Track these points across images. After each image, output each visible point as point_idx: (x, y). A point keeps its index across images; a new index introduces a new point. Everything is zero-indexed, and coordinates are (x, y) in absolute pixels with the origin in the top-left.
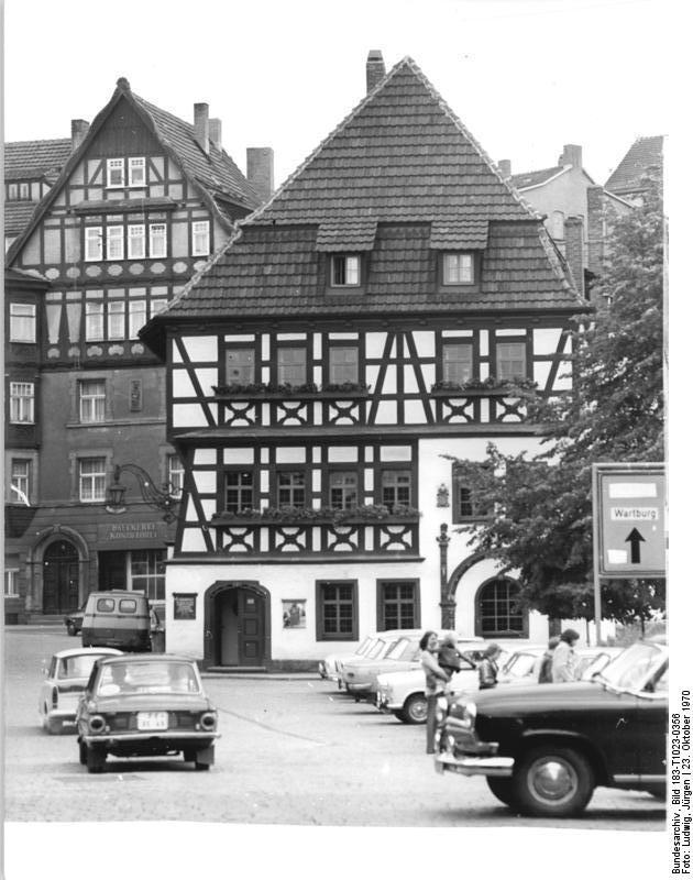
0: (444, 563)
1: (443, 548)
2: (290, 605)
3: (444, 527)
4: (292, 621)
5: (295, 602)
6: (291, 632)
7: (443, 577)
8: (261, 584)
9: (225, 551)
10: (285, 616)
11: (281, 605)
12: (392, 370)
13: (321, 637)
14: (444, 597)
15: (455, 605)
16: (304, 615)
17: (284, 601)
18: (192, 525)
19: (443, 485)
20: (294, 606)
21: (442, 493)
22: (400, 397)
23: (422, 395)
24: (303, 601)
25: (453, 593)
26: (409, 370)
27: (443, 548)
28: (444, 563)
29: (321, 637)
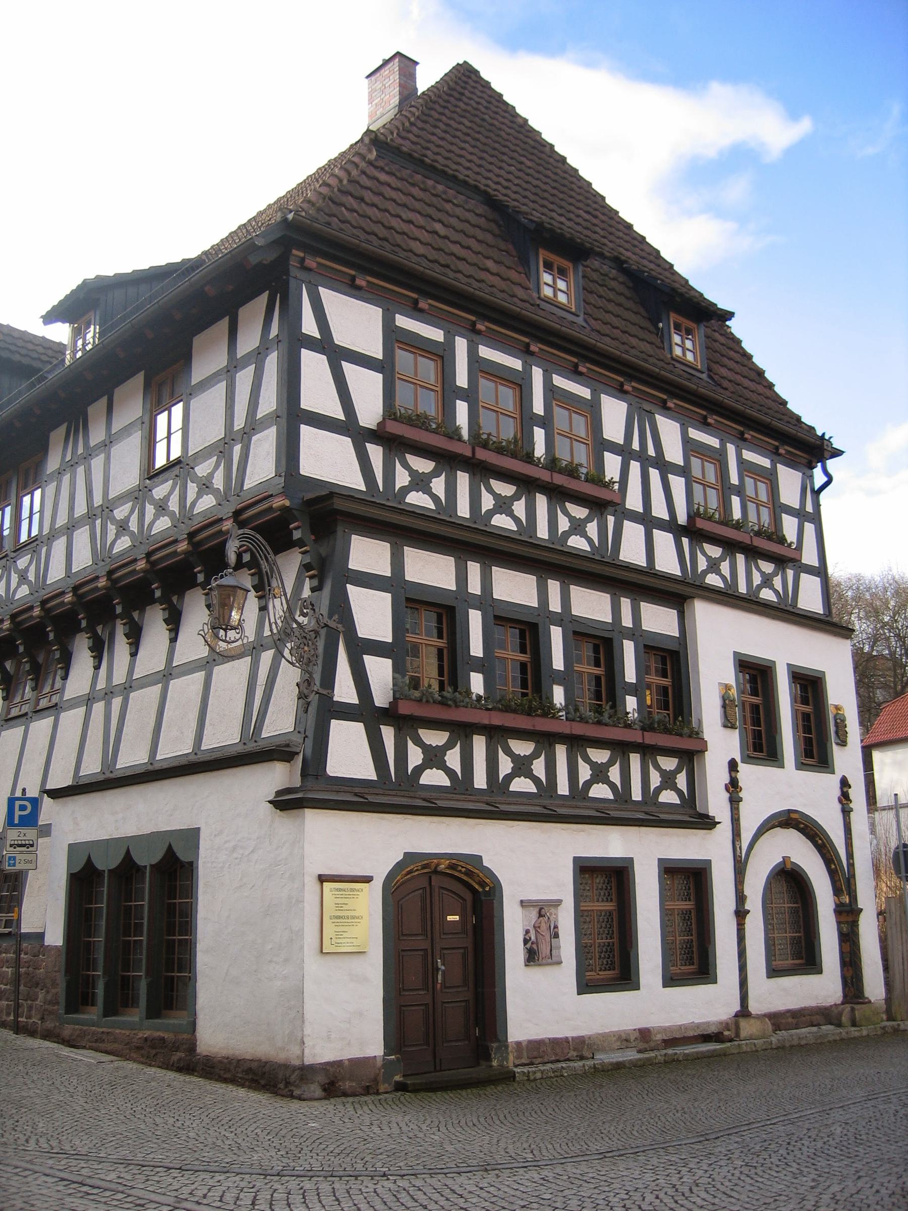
1: (735, 801)
2: (534, 913)
3: (733, 766)
6: (537, 974)
10: (526, 941)
11: (519, 909)
12: (635, 467)
13: (585, 986)
16: (556, 936)
18: (346, 713)
20: (541, 915)
21: (726, 704)
22: (646, 520)
23: (671, 526)
24: (557, 903)
26: (654, 474)
27: (735, 801)
29: (585, 986)
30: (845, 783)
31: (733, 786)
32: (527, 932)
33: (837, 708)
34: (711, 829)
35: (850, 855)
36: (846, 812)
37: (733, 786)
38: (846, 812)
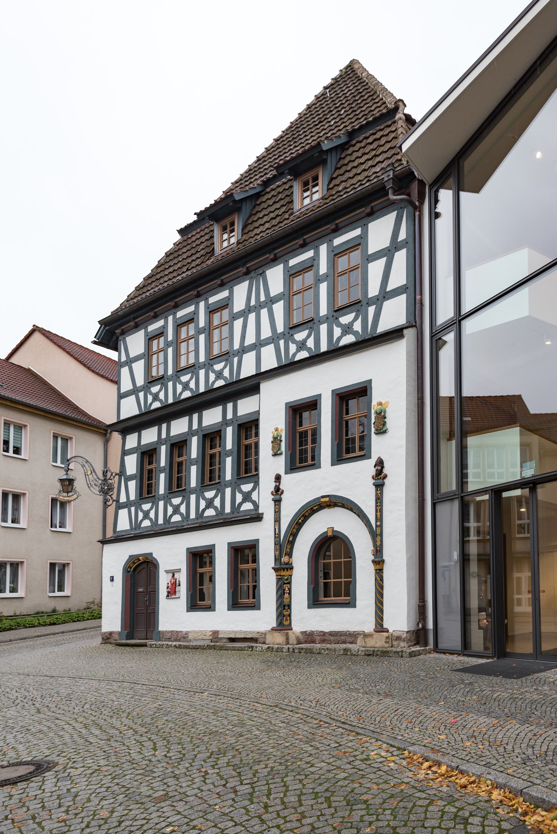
0: (277, 520)
1: (278, 502)
3: (278, 478)
4: (172, 592)
5: (173, 573)
6: (172, 603)
7: (277, 536)
8: (154, 556)
9: (138, 525)
10: (168, 588)
14: (277, 559)
15: (292, 568)
16: (179, 585)
17: (167, 572)
19: (277, 430)
21: (276, 440)
24: (179, 571)
25: (290, 555)
27: (278, 502)
28: (277, 520)
30: (380, 463)
31: (278, 491)
32: (168, 584)
33: (380, 404)
34: (261, 521)
35: (379, 518)
36: (379, 486)
37: (278, 491)
38: (379, 486)
